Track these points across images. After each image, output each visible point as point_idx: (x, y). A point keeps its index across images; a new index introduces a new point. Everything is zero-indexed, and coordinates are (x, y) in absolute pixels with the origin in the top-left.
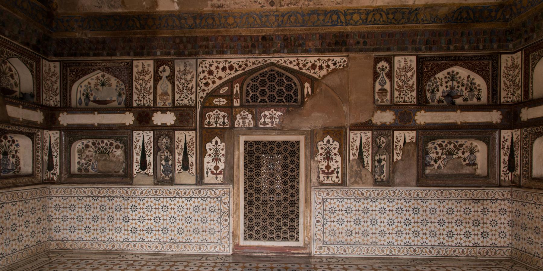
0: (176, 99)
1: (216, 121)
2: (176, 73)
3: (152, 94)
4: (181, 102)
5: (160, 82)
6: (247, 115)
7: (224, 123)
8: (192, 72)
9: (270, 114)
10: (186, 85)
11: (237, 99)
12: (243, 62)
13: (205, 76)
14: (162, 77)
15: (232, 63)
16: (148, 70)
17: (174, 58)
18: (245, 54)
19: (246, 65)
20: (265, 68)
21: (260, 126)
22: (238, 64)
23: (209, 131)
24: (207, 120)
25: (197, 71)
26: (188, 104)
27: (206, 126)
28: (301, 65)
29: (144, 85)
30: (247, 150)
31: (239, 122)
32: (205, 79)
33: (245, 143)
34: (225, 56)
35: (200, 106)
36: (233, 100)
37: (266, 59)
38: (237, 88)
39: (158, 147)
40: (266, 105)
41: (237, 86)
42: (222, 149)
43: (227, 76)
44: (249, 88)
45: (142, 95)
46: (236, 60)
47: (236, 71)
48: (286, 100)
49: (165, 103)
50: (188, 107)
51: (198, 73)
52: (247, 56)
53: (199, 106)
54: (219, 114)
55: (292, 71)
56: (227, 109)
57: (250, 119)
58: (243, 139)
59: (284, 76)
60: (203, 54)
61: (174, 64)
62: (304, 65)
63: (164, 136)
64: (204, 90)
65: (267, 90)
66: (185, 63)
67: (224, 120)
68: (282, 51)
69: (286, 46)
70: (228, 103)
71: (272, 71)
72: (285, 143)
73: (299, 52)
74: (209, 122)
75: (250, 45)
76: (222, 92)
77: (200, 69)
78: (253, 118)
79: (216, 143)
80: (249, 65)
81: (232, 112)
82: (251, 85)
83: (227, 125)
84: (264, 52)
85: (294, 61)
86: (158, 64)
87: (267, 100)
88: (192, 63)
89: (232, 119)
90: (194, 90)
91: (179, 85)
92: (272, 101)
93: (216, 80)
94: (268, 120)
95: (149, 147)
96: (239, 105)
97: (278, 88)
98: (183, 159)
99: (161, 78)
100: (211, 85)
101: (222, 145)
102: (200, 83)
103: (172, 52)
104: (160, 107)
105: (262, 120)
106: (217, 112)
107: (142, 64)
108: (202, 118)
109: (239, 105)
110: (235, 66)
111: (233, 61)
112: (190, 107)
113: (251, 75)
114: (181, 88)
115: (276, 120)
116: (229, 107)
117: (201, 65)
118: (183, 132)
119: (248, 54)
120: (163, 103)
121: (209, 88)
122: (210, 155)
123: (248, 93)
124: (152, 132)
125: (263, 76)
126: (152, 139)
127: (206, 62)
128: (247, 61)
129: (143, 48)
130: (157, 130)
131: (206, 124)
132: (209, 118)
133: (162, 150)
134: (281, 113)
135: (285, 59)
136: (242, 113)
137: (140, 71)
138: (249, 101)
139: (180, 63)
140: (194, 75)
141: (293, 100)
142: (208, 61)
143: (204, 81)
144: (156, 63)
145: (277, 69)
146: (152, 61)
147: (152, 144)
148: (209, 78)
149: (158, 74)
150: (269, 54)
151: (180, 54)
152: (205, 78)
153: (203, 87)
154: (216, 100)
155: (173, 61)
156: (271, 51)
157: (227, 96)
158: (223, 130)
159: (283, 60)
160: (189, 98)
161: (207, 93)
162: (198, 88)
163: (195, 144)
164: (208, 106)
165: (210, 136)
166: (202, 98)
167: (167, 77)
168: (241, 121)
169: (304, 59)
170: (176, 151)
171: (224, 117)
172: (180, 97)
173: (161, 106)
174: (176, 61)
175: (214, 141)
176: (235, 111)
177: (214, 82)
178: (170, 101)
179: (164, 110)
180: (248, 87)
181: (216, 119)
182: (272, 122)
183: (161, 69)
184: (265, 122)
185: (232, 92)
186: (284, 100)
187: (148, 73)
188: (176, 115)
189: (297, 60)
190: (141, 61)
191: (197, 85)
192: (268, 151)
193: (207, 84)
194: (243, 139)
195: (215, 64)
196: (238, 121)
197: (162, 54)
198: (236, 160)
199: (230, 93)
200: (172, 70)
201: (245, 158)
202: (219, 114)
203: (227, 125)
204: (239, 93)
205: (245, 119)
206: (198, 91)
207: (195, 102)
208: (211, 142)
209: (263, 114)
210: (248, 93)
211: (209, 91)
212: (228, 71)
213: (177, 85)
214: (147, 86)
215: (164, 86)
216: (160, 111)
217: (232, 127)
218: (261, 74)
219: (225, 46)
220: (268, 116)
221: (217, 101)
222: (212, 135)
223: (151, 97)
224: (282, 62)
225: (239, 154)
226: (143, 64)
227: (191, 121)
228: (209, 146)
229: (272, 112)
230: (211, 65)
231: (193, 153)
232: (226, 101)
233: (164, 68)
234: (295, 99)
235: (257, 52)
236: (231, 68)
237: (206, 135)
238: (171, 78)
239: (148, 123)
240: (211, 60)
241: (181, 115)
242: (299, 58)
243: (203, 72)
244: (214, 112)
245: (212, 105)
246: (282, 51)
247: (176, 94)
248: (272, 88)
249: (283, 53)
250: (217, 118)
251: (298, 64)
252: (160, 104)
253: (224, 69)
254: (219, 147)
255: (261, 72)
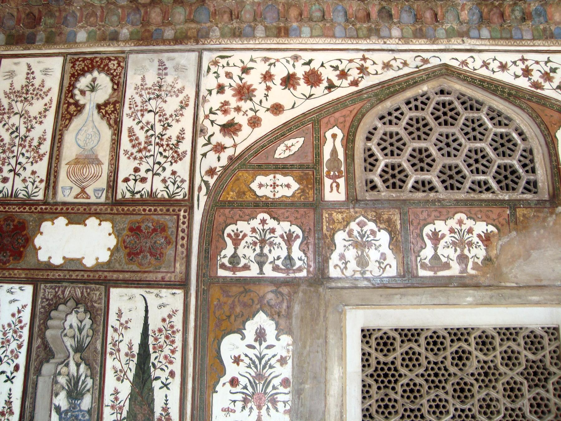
0: (121, 177)
1: (261, 255)
2: (130, 92)
3: (46, 159)
4: (139, 186)
5: (76, 123)
6: (373, 233)
7: (289, 258)
8: (180, 91)
9: (452, 231)
10: (159, 129)
11: (334, 178)
12: (351, 61)
13: (226, 103)
14: (83, 106)
15: (315, 65)
16: (42, 85)
17: (127, 49)
18: (358, 37)
19: (362, 70)
20: (423, 81)
21: (422, 273)
22: (336, 68)
23: (235, 290)
24: (229, 251)
25: (198, 86)
26: (162, 193)
27: (222, 273)
28: (536, 76)
29: (23, 131)
30: (373, 362)
31: (343, 261)
32: (225, 112)
33: (366, 334)
34: (294, 43)
35: (203, 199)
36: (320, 182)
37: (425, 55)
38: (333, 142)
39: (45, 345)
40: (434, 202)
41: (334, 136)
42: (283, 361)
43: (300, 102)
44: (373, 145)
45: (13, 161)
46: (330, 55)
47: (331, 87)
48: (499, 182)
49: (83, 190)
50: (162, 202)
51: (203, 92)
52: (364, 44)
53: (201, 200)
54: (273, 231)
55: (511, 94)
56: (302, 211)
57: (385, 248)
58: (356, 320)
59: (485, 110)
60: (223, 36)
61: (125, 68)
62: (547, 77)
63: (71, 303)
64: (220, 148)
65: (433, 151)
66: (161, 63)
67: (289, 249)
68: (474, 33)
69: (483, 21)
70: (303, 191)
71: (442, 92)
72: (508, 333)
73: (528, 35)
74: (234, 258)
75: (374, 12)
76: (281, 152)
77: (210, 82)
78: (394, 244)
79: (260, 336)
80: (371, 70)
81: (318, 222)
82: (379, 134)
83: (300, 270)
84: (419, 34)
85: (514, 63)
86: (79, 67)
87: (436, 183)
88: (183, 62)
89: (321, 247)
90: (185, 146)
91: (137, 129)
92: (452, 187)
93: (262, 113)
94: (447, 252)
95: (13, 345)
96: (341, 197)
97: (468, 145)
98: (132, 397)
99: (80, 108)
100: (246, 129)
101: (283, 345)
102: (207, 123)
103: (125, 32)
104: (64, 204)
105: (428, 253)
106: (263, 222)
107: (26, 70)
108: (210, 243)
109: (341, 197)
110: (328, 74)
111: (318, 58)
112: (170, 203)
113: (381, 101)
114: (142, 139)
115: (474, 251)
116: (305, 205)
117: (213, 69)
118: (137, 292)
119: (368, 37)
120: (76, 190)
121: (238, 139)
122: (234, 382)
123: (370, 161)
124: (29, 289)
125: (416, 108)
126: (26, 316)
127: (231, 61)
128: (364, 59)
129: (34, 21)
130: (46, 281)
131: (223, 266)
132: (236, 244)
133: (59, 357)
134: (491, 228)
135: (486, 56)
136: (353, 226)
137: (18, 87)
138: (374, 188)
139: (147, 63)
140: (188, 98)
141: (523, 183)
142: (236, 58)
143: (222, 119)
144: (69, 66)
145: (458, 86)
146: (60, 60)
147: (25, 333)
148: (238, 109)
149: (72, 97)
150: (434, 40)
151: (147, 38)
152: (224, 108)
153: (219, 138)
154: (260, 179)
155: (125, 59)
156: (441, 32)
157: (301, 166)
158: (285, 290)
159: (479, 58)
160: (167, 174)
161: (230, 158)
162: (201, 141)
163: (178, 337)
164: (231, 200)
165: (238, 310)
166: (211, 172)
167: (99, 107)
168: (351, 254)
169: (544, 57)
170: (110, 362)
171: (289, 239)
172: (136, 170)
173: (70, 199)
174: (132, 57)
175: (251, 327)
176: (331, 221)
177: (255, 122)
178: (102, 183)
179: (77, 213)
180: (368, 139)
181: (263, 247)
182: (463, 259)
183: (84, 82)
184: (436, 257)
185: (319, 154)
186: (493, 184)
187: (40, 92)
188: (117, 232)
189: (523, 60)
190: (24, 61)
191: (197, 130)
192: (448, 363)
193: (230, 128)
194: (356, 320)
195: (262, 68)
196: (342, 257)
197: (92, 39)
198: (332, 401)
199: (309, 159)
200: (119, 85)
201: (366, 394)
202: (273, 231)
203: (300, 270)
204: (341, 156)
205: (363, 251)
206: (200, 150)
207: (186, 185)
208: (240, 331)
209: (428, 230)
210: (370, 161)
211: (239, 150)
212: (303, 88)
213: (131, 130)
214: (32, 134)
215: (88, 133)
216: (65, 214)
217: (320, 277)
218: (408, 103)
219: (293, 13)
220: (448, 239)
221: (263, 186)
222: (245, 305)
223: (42, 168)
224: (474, 64)
225: (343, 378)
226: (29, 67)
227: (169, 252)
228: (231, 346)
229: (460, 222)
230: (246, 70)
231: (172, 374)
232: (295, 186)
233: (94, 80)
234: (528, 183)
235: (396, 32)
236: (313, 78)
237: (223, 305)
238: (111, 111)
239: (18, 255)
240: (246, 56)
241: (135, 230)
242: (526, 56)
243: (221, 89)
244: (255, 223)
245: (249, 197)
246: (474, 33)
247: (123, 158)
248: (449, 145)
249: (479, 38)
250: (263, 242)
251: (527, 72)
252: (66, 191)
253: (289, 81)
254: (270, 352)
255: (409, 94)
